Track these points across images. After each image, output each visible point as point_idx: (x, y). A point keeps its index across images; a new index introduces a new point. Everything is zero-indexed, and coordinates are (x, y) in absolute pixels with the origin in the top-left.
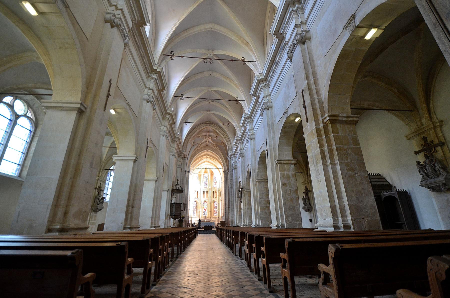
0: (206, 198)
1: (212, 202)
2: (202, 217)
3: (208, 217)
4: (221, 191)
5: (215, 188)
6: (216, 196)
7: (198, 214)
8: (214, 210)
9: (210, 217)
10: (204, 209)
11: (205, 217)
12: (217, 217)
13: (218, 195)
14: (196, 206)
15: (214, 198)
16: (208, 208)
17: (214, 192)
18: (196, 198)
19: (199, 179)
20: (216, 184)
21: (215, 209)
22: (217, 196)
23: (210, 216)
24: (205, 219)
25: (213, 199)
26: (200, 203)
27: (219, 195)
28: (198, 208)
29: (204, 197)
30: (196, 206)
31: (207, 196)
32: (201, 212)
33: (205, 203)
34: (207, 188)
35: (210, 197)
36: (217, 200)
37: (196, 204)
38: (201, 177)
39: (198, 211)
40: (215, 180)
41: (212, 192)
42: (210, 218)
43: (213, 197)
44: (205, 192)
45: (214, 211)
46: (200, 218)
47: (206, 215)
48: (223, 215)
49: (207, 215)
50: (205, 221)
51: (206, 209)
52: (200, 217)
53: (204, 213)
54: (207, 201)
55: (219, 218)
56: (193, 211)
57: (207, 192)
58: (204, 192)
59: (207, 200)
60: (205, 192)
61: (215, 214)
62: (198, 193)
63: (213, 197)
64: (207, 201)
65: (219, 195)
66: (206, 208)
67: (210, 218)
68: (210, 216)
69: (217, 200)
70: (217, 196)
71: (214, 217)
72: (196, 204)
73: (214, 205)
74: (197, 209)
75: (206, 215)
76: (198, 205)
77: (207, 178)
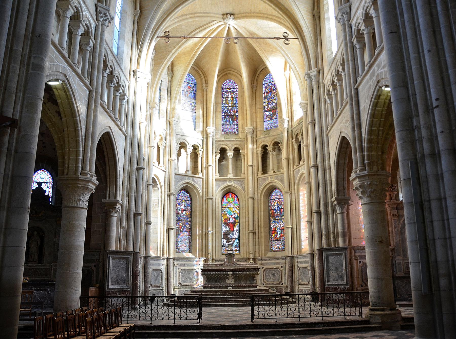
0: (231, 175)
1: (261, 189)
2: (218, 256)
3: (244, 255)
4: (300, 138)
5: (270, 130)
6: (276, 166)
7: (198, 242)
8: (270, 228)
9: (252, 256)
10: (227, 224)
11: (230, 256)
12: (287, 257)
13: (288, 159)
14: (191, 212)
15: (270, 173)
16: (242, 220)
17: (270, 148)
18: (190, 173)
19: (199, 96)
20: (274, 114)
21: (273, 224)
22: (284, 163)
23: (251, 251)
24: (229, 266)
25: (264, 180)
26: (204, 199)
27: (291, 157)
28: (198, 220)
29: (222, 170)
30: (191, 212)
31: (237, 169)
32: (210, 236)
33: (230, 198)
34: (234, 133)
35: (250, 168)
36: (282, 181)
37: (191, 200)
38: (207, 87)
39: (198, 231)
40: (271, 100)
41: (260, 150)
42: (254, 260)
43: (265, 171)
44: (230, 154)
45: (271, 231)
46: (206, 260)
47: (235, 249)
48: (329, 244)
49: (238, 249)
50: (230, 273)
51: (234, 223)
52: (210, 257)
53: (225, 241)
54: (239, 188)
55: (296, 260)
56: (172, 232)
57: (237, 151)
58: (223, 151)
59: (236, 185)
60: (230, 154)
61: (277, 245)
62: (195, 156)
63: (265, 171)
64: (239, 188)
65: (291, 157)
66: (232, 220)
67: (251, 261)
68: (254, 252)
69: (282, 181)
70: (284, 163)
71: (270, 255)
72: (191, 200)
73: (269, 206)
74: (194, 221)
75: (234, 248)
76: (198, 203)
77: (233, 95)
